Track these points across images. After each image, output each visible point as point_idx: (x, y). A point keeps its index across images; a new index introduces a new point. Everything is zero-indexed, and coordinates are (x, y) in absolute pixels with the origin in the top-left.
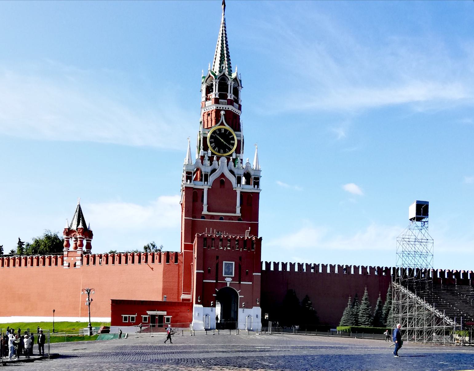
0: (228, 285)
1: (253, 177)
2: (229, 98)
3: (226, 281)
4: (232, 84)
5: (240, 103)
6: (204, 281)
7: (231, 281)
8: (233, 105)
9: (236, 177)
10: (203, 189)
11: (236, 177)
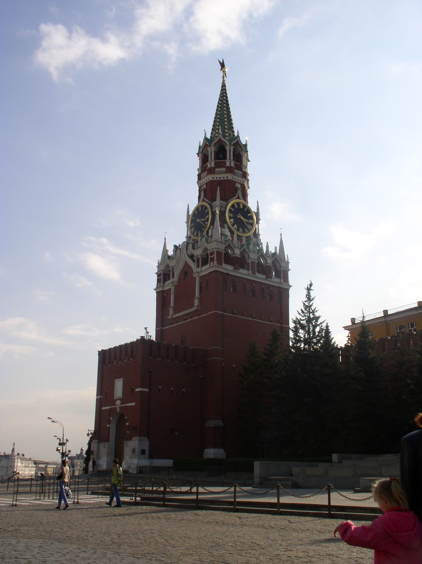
0: (118, 410)
1: (208, 252)
2: (209, 166)
3: (115, 405)
4: (213, 150)
5: (228, 164)
6: (103, 408)
7: (121, 404)
8: (214, 173)
9: (196, 260)
10: (170, 289)
11: (196, 260)
